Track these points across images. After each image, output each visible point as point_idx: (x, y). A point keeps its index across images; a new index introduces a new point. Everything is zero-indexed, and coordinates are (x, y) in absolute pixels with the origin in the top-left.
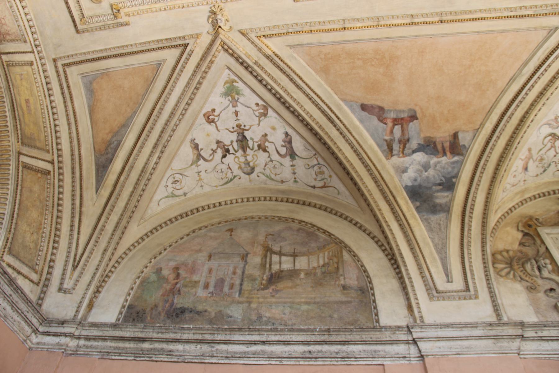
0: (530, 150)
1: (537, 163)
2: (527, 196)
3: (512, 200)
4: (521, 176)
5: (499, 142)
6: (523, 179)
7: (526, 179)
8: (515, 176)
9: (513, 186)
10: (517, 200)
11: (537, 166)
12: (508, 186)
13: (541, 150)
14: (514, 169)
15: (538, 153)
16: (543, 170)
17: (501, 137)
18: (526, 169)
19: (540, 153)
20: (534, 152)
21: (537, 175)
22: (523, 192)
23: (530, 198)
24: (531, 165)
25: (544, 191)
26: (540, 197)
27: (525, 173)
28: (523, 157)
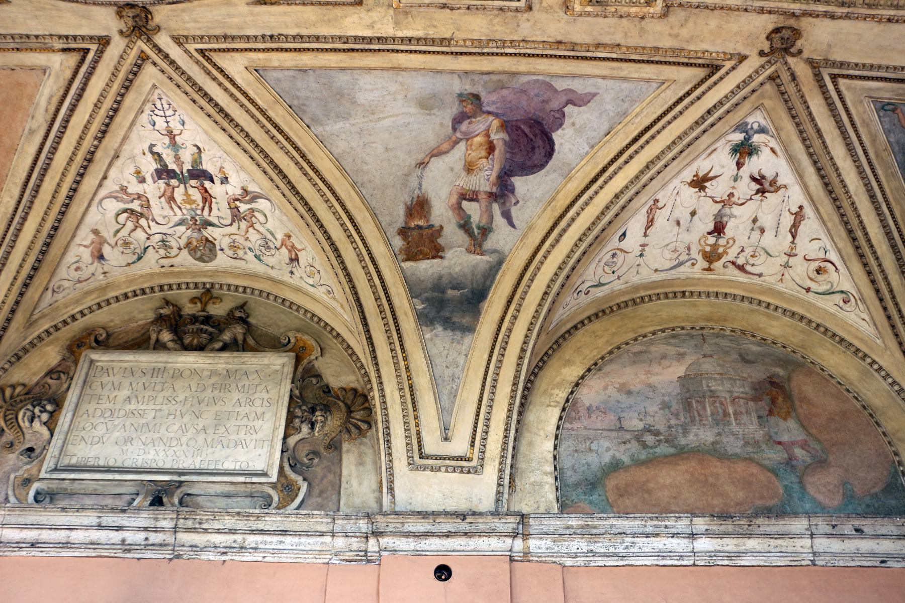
0: (96, 232)
1: (121, 249)
2: (112, 294)
3: (77, 302)
4: (92, 268)
5: (27, 224)
6: (102, 271)
7: (106, 269)
8: (78, 269)
9: (80, 282)
10: (90, 301)
11: (122, 253)
12: (66, 284)
13: (118, 231)
14: (70, 258)
15: (115, 235)
16: (136, 256)
17: (30, 218)
18: (101, 257)
19: (120, 235)
20: (107, 234)
21: (129, 265)
22: (103, 289)
23: (117, 297)
24: (106, 250)
25: (145, 286)
26: (136, 295)
27: (100, 262)
28: (87, 243)
